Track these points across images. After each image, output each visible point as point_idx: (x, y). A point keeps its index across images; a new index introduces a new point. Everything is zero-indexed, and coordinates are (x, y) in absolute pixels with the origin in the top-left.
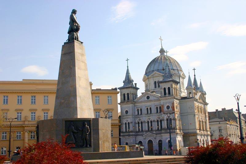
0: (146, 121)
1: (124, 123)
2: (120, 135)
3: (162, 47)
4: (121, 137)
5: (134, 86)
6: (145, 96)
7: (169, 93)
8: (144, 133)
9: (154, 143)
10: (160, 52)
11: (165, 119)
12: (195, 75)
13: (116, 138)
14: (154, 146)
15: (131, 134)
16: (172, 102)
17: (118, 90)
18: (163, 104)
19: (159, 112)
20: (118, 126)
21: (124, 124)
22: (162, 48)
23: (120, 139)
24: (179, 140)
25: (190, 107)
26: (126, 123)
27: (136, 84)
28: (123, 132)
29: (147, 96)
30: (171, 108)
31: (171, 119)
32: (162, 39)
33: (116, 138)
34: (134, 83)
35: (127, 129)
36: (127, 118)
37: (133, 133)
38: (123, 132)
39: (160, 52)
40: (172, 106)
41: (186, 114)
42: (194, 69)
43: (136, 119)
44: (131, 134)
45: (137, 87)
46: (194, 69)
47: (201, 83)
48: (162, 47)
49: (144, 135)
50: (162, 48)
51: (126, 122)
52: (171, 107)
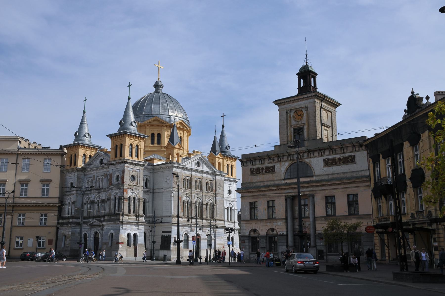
0: (96, 201)
1: (67, 203)
2: (58, 223)
4: (59, 226)
6: (98, 159)
7: (121, 155)
8: (91, 220)
9: (100, 237)
11: (112, 197)
13: (52, 226)
14: (100, 241)
15: (71, 220)
16: (122, 170)
17: (65, 150)
18: (111, 173)
20: (57, 209)
21: (66, 204)
22: (158, 80)
23: (58, 229)
24: (129, 235)
25: (168, 178)
26: (69, 203)
28: (64, 218)
29: (100, 158)
30: (121, 178)
31: (119, 197)
36: (71, 195)
37: (75, 220)
38: (64, 218)
40: (121, 174)
41: (161, 190)
42: (223, 116)
43: (84, 197)
44: (71, 220)
46: (223, 116)
49: (88, 224)
50: (158, 80)
52: (121, 177)
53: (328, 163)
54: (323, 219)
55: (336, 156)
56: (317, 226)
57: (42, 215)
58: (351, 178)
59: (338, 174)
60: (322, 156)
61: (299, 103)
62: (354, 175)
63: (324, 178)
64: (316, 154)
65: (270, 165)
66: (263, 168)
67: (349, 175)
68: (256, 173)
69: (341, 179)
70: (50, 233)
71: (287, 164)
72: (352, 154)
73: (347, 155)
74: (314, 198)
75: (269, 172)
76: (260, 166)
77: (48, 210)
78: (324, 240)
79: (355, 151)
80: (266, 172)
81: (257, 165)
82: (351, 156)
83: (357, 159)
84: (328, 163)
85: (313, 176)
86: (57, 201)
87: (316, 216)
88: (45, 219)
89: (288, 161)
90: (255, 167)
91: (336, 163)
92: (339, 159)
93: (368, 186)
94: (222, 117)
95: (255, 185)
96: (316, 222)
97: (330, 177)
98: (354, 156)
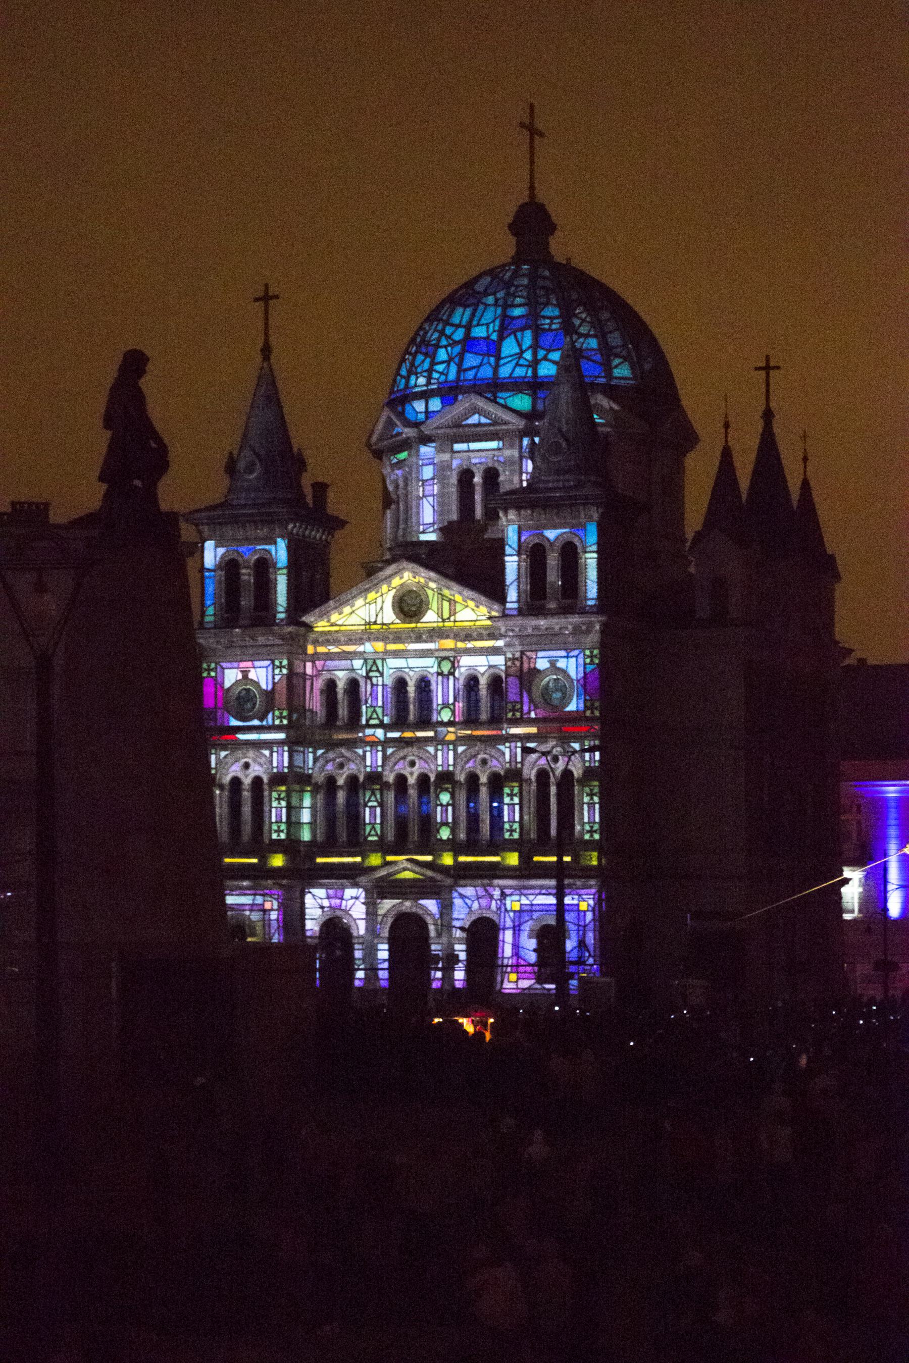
1: (227, 779)
3: (532, 188)
5: (309, 500)
10: (515, 234)
12: (768, 415)
19: (484, 717)
22: (532, 196)
27: (320, 489)
32: (539, 125)
34: (307, 481)
35: (247, 829)
39: (516, 228)
42: (767, 368)
45: (335, 505)
47: (805, 485)
48: (532, 188)
50: (532, 196)
51: (235, 770)
94: (763, 373)
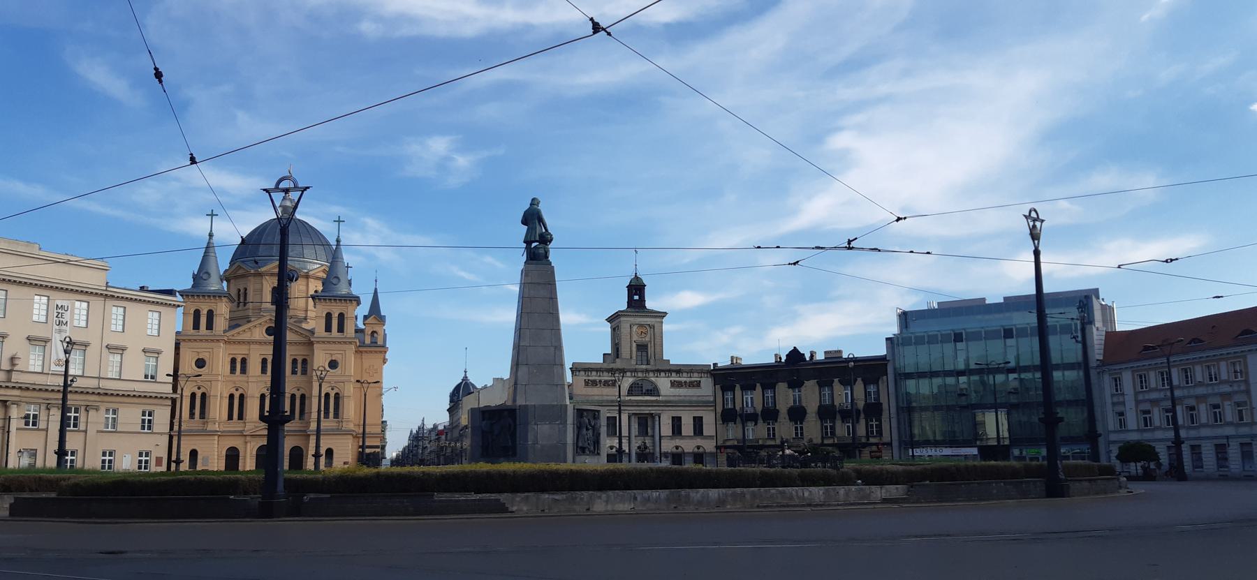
20: (169, 402)
33: (161, 434)
53: (673, 384)
54: (669, 438)
55: (683, 380)
56: (662, 444)
57: (144, 414)
58: (696, 402)
59: (685, 396)
60: (668, 377)
61: (645, 319)
62: (700, 399)
63: (672, 398)
64: (663, 374)
65: (610, 379)
66: (600, 381)
67: (694, 399)
68: (592, 385)
69: (691, 402)
70: (158, 445)
71: (631, 380)
72: (699, 379)
73: (693, 379)
74: (659, 417)
75: (609, 385)
76: (597, 378)
77: (121, 403)
78: (669, 458)
79: (701, 377)
80: (604, 385)
81: (594, 376)
82: (696, 381)
83: (702, 384)
84: (673, 384)
85: (659, 396)
86: (169, 389)
87: (662, 435)
88: (150, 421)
89: (632, 377)
90: (590, 378)
91: (682, 386)
92: (685, 382)
93: (712, 410)
95: (590, 399)
96: (662, 441)
97: (677, 398)
98: (700, 381)
